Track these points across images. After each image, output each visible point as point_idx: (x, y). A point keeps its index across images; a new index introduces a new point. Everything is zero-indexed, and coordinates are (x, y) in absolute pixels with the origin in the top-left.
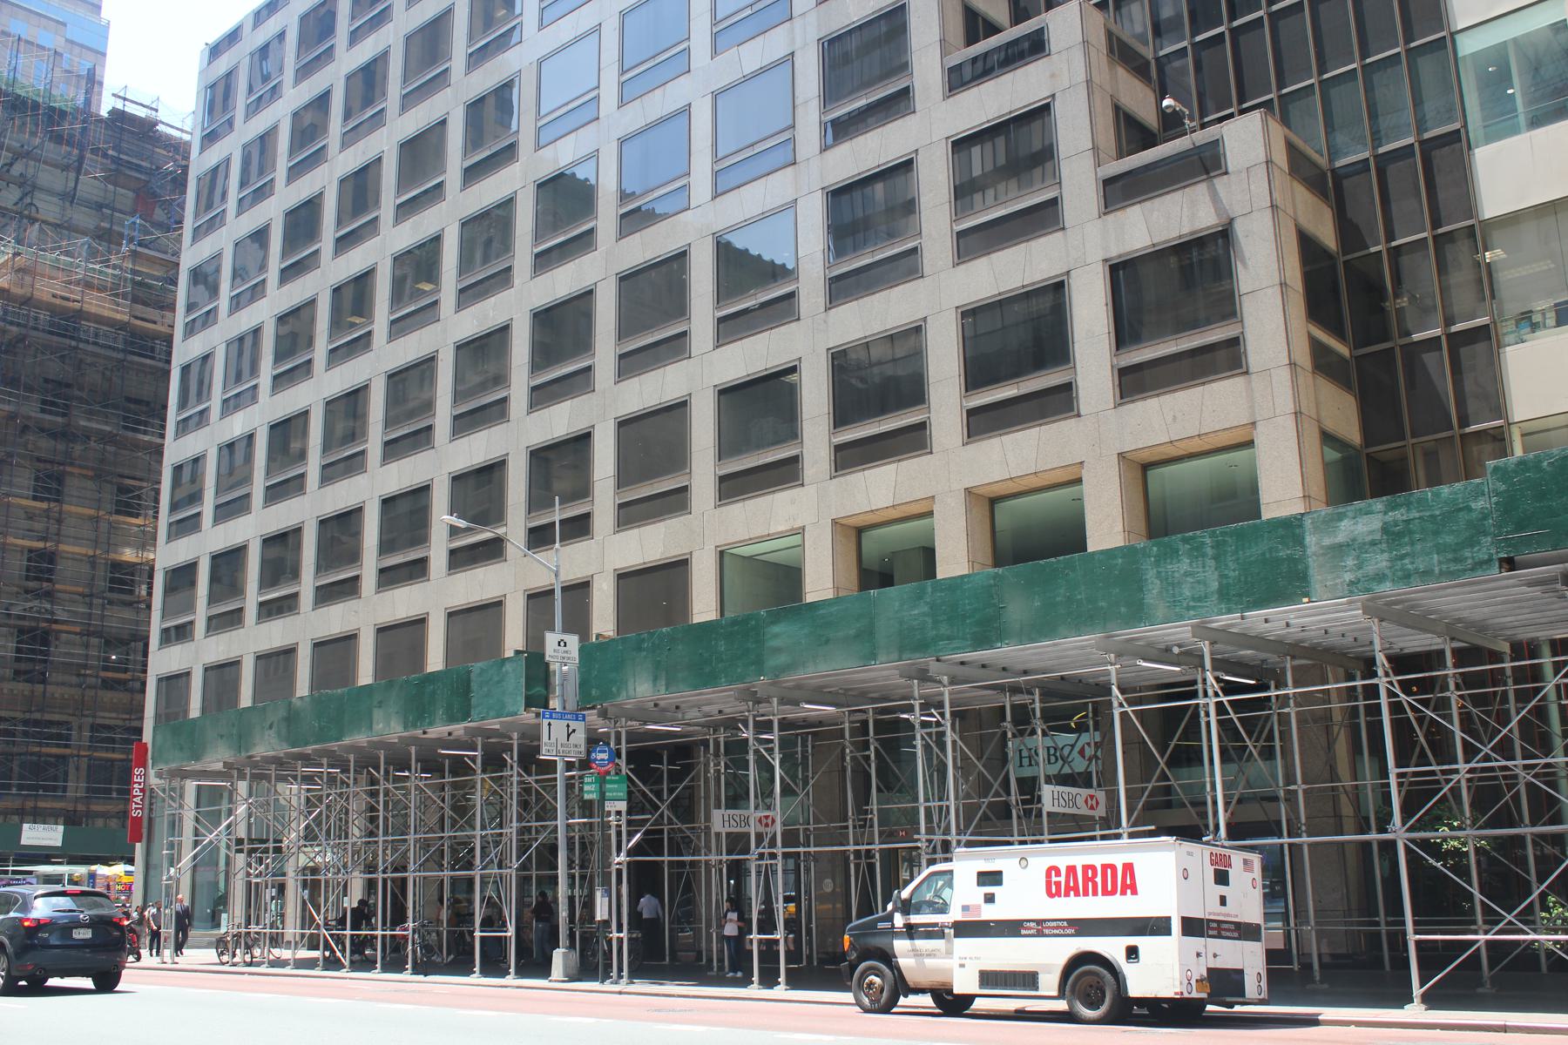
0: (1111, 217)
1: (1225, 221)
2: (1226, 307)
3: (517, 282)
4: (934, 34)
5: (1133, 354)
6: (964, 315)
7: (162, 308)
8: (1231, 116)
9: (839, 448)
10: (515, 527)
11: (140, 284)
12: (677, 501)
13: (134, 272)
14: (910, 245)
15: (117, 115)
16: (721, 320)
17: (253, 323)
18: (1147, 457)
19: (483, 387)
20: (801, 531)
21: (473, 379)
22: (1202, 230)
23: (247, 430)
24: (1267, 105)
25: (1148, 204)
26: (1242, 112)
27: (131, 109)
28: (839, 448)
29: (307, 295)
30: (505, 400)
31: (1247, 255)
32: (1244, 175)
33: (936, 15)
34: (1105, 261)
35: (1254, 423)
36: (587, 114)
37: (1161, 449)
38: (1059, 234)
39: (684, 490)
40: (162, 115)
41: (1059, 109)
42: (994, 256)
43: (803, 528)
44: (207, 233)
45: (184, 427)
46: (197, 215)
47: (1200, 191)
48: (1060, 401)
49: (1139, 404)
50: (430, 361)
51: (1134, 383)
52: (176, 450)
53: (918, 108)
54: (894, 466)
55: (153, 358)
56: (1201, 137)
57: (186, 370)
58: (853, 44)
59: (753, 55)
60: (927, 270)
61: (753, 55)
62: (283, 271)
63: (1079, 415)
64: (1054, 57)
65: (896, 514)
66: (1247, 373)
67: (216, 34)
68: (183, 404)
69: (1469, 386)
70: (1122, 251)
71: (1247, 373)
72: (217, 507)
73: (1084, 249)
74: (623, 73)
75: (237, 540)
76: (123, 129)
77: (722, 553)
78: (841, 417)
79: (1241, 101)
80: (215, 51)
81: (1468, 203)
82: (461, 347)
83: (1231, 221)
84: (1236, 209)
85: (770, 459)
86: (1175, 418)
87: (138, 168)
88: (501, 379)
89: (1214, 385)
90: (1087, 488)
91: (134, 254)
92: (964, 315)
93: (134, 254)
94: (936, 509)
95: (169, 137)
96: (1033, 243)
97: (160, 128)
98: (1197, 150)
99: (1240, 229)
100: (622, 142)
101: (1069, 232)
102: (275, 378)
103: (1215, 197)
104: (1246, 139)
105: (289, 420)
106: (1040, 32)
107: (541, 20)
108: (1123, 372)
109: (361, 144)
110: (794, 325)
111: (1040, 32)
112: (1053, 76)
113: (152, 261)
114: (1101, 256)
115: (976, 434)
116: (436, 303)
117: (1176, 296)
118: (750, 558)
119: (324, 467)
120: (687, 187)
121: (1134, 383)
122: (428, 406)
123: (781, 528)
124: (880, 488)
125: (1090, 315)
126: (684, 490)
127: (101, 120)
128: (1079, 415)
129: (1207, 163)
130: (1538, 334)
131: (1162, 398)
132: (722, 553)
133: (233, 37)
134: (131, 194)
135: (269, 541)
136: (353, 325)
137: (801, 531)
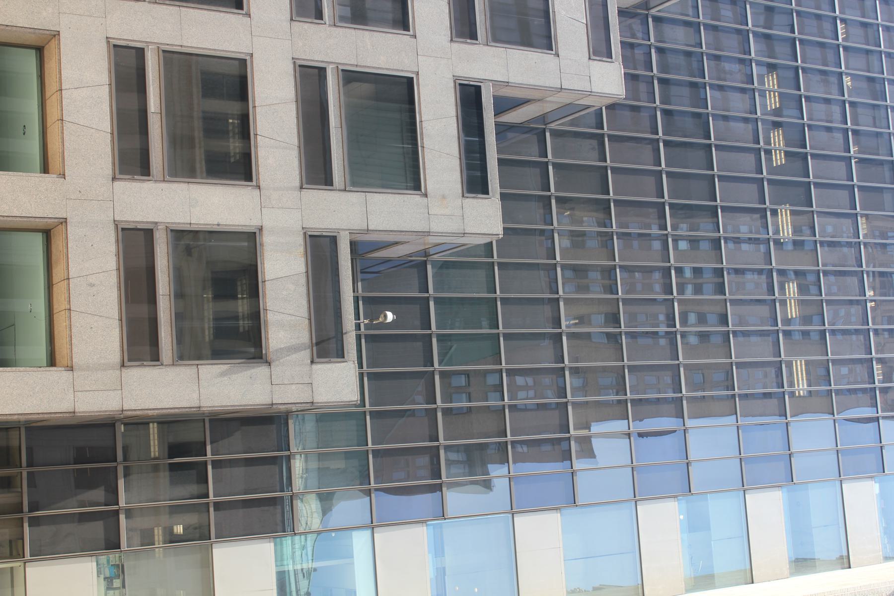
0: (300, 240)
1: (271, 356)
2: (183, 168)
4: (515, 78)
5: (165, 262)
6: (243, 62)
8: (361, 366)
18: (57, 244)
22: (267, 332)
25: (303, 280)
26: (361, 376)
31: (234, 376)
32: (307, 380)
33: (532, 82)
34: (261, 229)
35: (71, 368)
38: (297, 183)
41: (412, 199)
42: (293, 107)
48: (133, 161)
49: (113, 248)
51: (136, 242)
53: (455, 46)
56: (350, 341)
64: (459, 201)
66: (123, 365)
69: (67, 528)
71: (123, 365)
73: (277, 209)
79: (373, 376)
81: (229, 534)
83: (269, 363)
84: (276, 369)
86: (92, 285)
89: (116, 333)
90: (36, 179)
92: (243, 62)
98: (340, 334)
99: (259, 371)
103: (294, 349)
104: (339, 383)
106: (485, 190)
108: (148, 234)
111: (485, 190)
112: (444, 197)
114: (267, 224)
115: (116, 55)
117: (208, 295)
121: (136, 242)
129: (326, 345)
130: (103, 584)
131: (115, 273)
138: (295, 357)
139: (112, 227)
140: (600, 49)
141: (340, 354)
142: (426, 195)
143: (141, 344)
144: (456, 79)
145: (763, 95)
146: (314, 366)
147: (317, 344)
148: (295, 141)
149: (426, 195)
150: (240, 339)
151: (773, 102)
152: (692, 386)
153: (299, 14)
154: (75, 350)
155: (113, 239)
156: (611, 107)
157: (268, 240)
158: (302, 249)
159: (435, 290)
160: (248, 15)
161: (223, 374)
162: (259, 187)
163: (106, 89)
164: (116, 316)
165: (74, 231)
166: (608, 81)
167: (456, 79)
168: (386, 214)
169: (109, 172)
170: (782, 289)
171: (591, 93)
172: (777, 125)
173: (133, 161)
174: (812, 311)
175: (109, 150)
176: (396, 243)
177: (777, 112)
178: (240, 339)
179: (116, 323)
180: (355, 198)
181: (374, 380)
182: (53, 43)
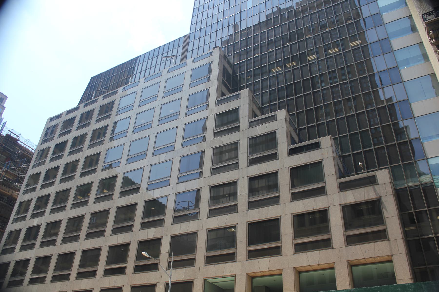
0: (342, 193)
1: (378, 197)
3: (141, 191)
4: (285, 140)
5: (355, 231)
6: (294, 216)
7: (10, 188)
8: (377, 170)
9: (249, 252)
10: (130, 264)
11: (5, 180)
12: (191, 262)
13: (5, 177)
14: (276, 195)
15: (8, 135)
16: (210, 210)
17: (48, 193)
18: (355, 263)
19: (125, 220)
20: (235, 276)
21: (123, 217)
22: (371, 199)
23: (39, 223)
24: (388, 168)
25: (354, 191)
26: (379, 169)
27: (12, 135)
28: (249, 252)
29: (68, 187)
30: (132, 226)
32: (384, 185)
34: (341, 205)
35: (392, 255)
36: (170, 149)
37: (361, 261)
38: (325, 196)
39: (194, 259)
40: (20, 139)
41: (325, 163)
42: (304, 200)
43: (236, 275)
44: (37, 166)
45: (16, 220)
46: (35, 161)
47: (370, 188)
49: (353, 247)
50: (107, 211)
51: (350, 240)
52: (11, 227)
53: (279, 158)
54: (269, 258)
55: (3, 201)
56: (369, 174)
57: (21, 204)
58: (259, 141)
59: (163, 157)
60: (281, 202)
61: (194, 149)
62: (61, 179)
63: (333, 248)
64: (323, 150)
65: (267, 273)
67: (52, 116)
68: (18, 213)
70: (346, 203)
72: (22, 246)
74: (184, 139)
75: (27, 257)
76: (8, 140)
77: (205, 280)
78: (251, 242)
79: (379, 166)
80: (52, 119)
82: (119, 208)
85: (221, 253)
86: (365, 252)
87: (10, 151)
88: (132, 219)
89: (379, 243)
91: (6, 171)
92: (294, 216)
93: (6, 171)
94: (283, 273)
95: (20, 145)
96: (317, 198)
97: (19, 142)
99: (383, 199)
100: (181, 157)
101: (328, 196)
102: (52, 209)
103: (375, 191)
104: (383, 176)
105: (57, 222)
107: (159, 123)
109: (95, 148)
110: (236, 214)
112: (322, 154)
113: (11, 174)
114: (339, 203)
116: (112, 194)
118: (211, 283)
119: (64, 238)
120: (170, 180)
122: (105, 224)
123: (227, 274)
124: (263, 265)
125: (336, 220)
126: (194, 259)
127: (3, 136)
128: (333, 248)
131: (361, 245)
132: (205, 280)
133: (58, 117)
134: (5, 157)
135: (38, 259)
136: (78, 198)
137: (235, 276)
138: (377, 190)
139: (347, 247)
140: (273, 118)
141: (374, 177)
142: (323, 159)
143: (382, 235)
144: (288, 156)
145: (277, 72)
146: (379, 183)
147: (372, 184)
148: (314, 198)
149: (323, 159)
150: (374, 207)
151: (279, 69)
152: (365, 73)
153: (278, 202)
154: (386, 255)
155: (351, 247)
156: (289, 112)
157: (343, 202)
158: (344, 192)
159: (350, 152)
160: (281, 216)
161: (386, 210)
162: (328, 207)
163: (307, 253)
164: (374, 243)
165: (350, 259)
166: (281, 114)
167: (288, 156)
168: (330, 170)
169: (331, 250)
170: (331, 54)
171: (286, 118)
172: (285, 66)
173: (327, 244)
174: (336, 45)
175: (325, 251)
176: (338, 165)
177: (282, 67)
178: (374, 207)
179: (376, 243)
180: (327, 179)
181: (381, 165)
182: (297, 269)
